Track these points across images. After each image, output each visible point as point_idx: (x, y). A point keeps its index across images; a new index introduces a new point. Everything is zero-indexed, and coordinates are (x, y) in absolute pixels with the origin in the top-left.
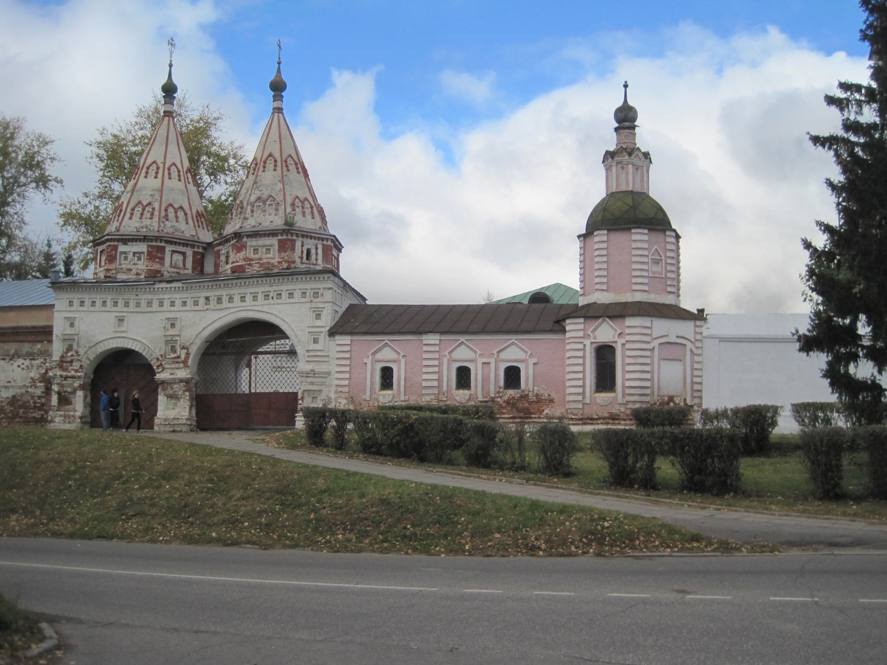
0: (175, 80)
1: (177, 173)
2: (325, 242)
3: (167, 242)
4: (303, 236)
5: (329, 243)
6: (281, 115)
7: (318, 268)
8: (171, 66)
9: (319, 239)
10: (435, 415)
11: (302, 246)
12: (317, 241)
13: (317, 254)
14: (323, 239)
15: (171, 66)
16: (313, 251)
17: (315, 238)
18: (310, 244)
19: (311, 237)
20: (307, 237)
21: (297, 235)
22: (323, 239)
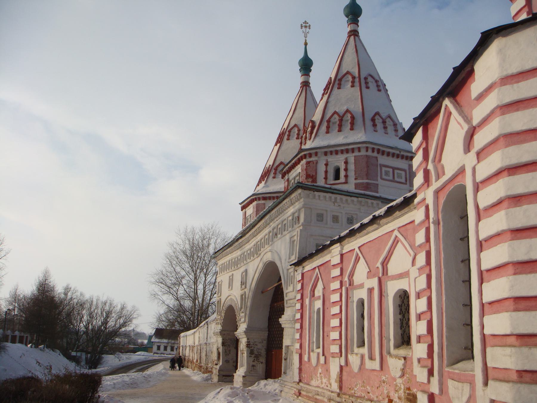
0: (310, 55)
1: (297, 132)
2: (356, 153)
3: (265, 199)
4: (326, 154)
5: (363, 153)
6: (356, 37)
7: (350, 187)
8: (306, 44)
9: (347, 151)
10: (325, 391)
11: (326, 165)
12: (345, 156)
13: (346, 170)
14: (353, 150)
15: (306, 44)
16: (342, 167)
17: (342, 152)
18: (338, 161)
19: (337, 152)
20: (331, 153)
21: (316, 154)
22: (353, 150)
